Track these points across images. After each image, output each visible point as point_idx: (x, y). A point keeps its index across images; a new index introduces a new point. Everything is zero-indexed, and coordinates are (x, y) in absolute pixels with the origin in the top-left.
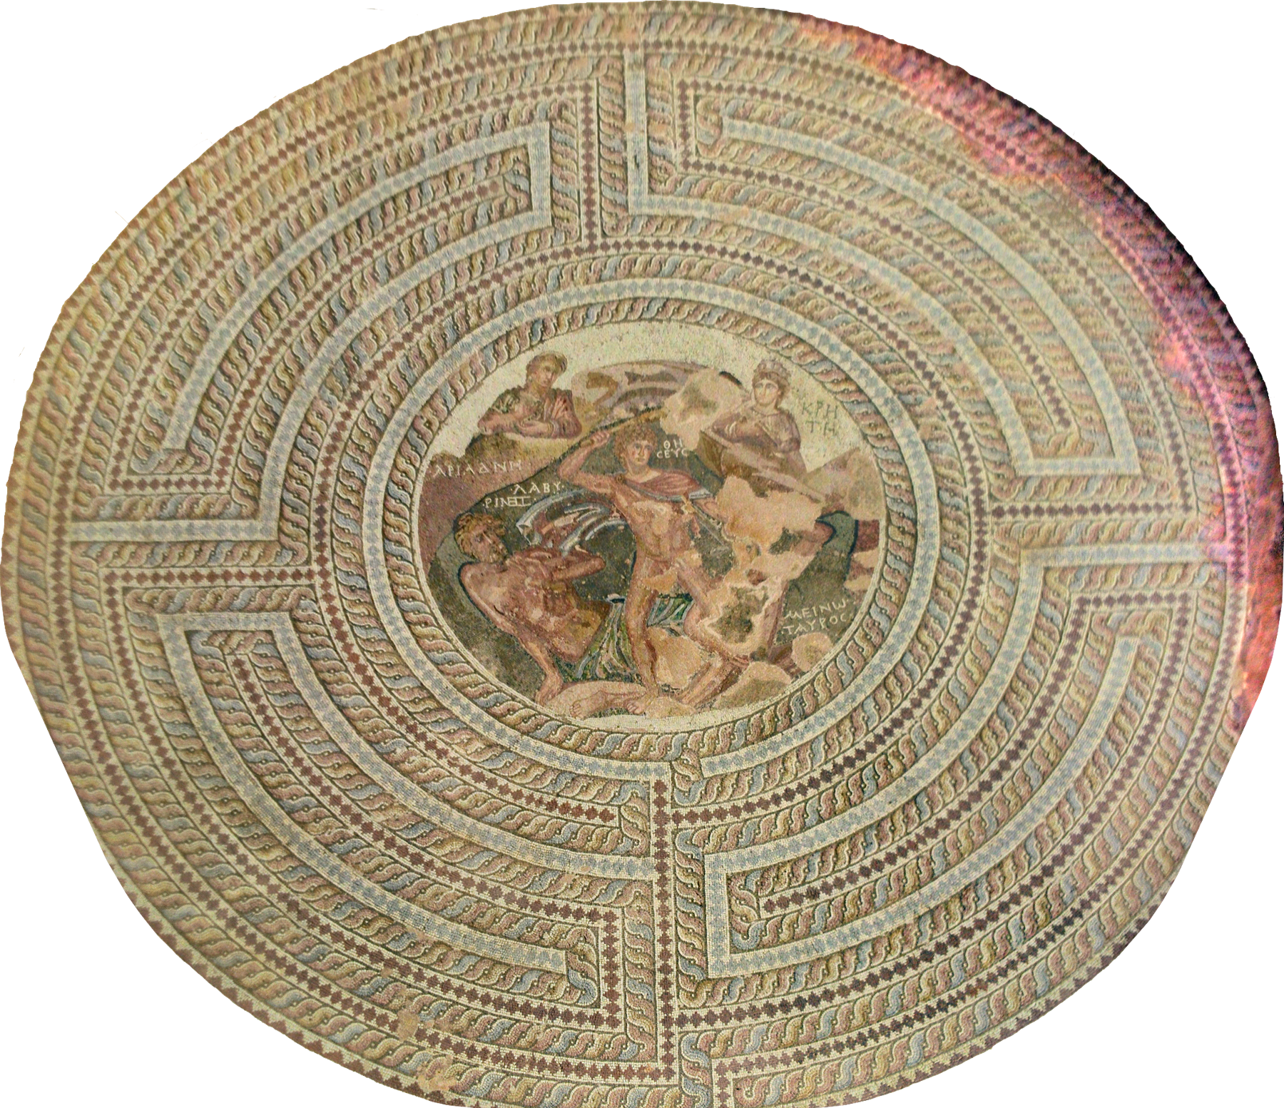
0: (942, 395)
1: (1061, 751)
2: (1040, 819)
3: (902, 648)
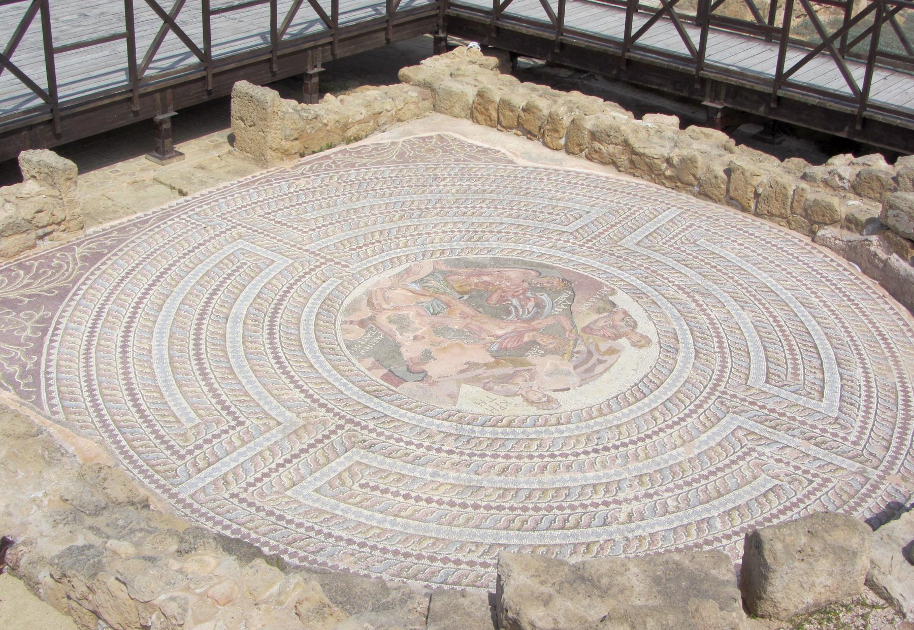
0: (450, 452)
1: (174, 369)
2: (154, 343)
3: (309, 356)
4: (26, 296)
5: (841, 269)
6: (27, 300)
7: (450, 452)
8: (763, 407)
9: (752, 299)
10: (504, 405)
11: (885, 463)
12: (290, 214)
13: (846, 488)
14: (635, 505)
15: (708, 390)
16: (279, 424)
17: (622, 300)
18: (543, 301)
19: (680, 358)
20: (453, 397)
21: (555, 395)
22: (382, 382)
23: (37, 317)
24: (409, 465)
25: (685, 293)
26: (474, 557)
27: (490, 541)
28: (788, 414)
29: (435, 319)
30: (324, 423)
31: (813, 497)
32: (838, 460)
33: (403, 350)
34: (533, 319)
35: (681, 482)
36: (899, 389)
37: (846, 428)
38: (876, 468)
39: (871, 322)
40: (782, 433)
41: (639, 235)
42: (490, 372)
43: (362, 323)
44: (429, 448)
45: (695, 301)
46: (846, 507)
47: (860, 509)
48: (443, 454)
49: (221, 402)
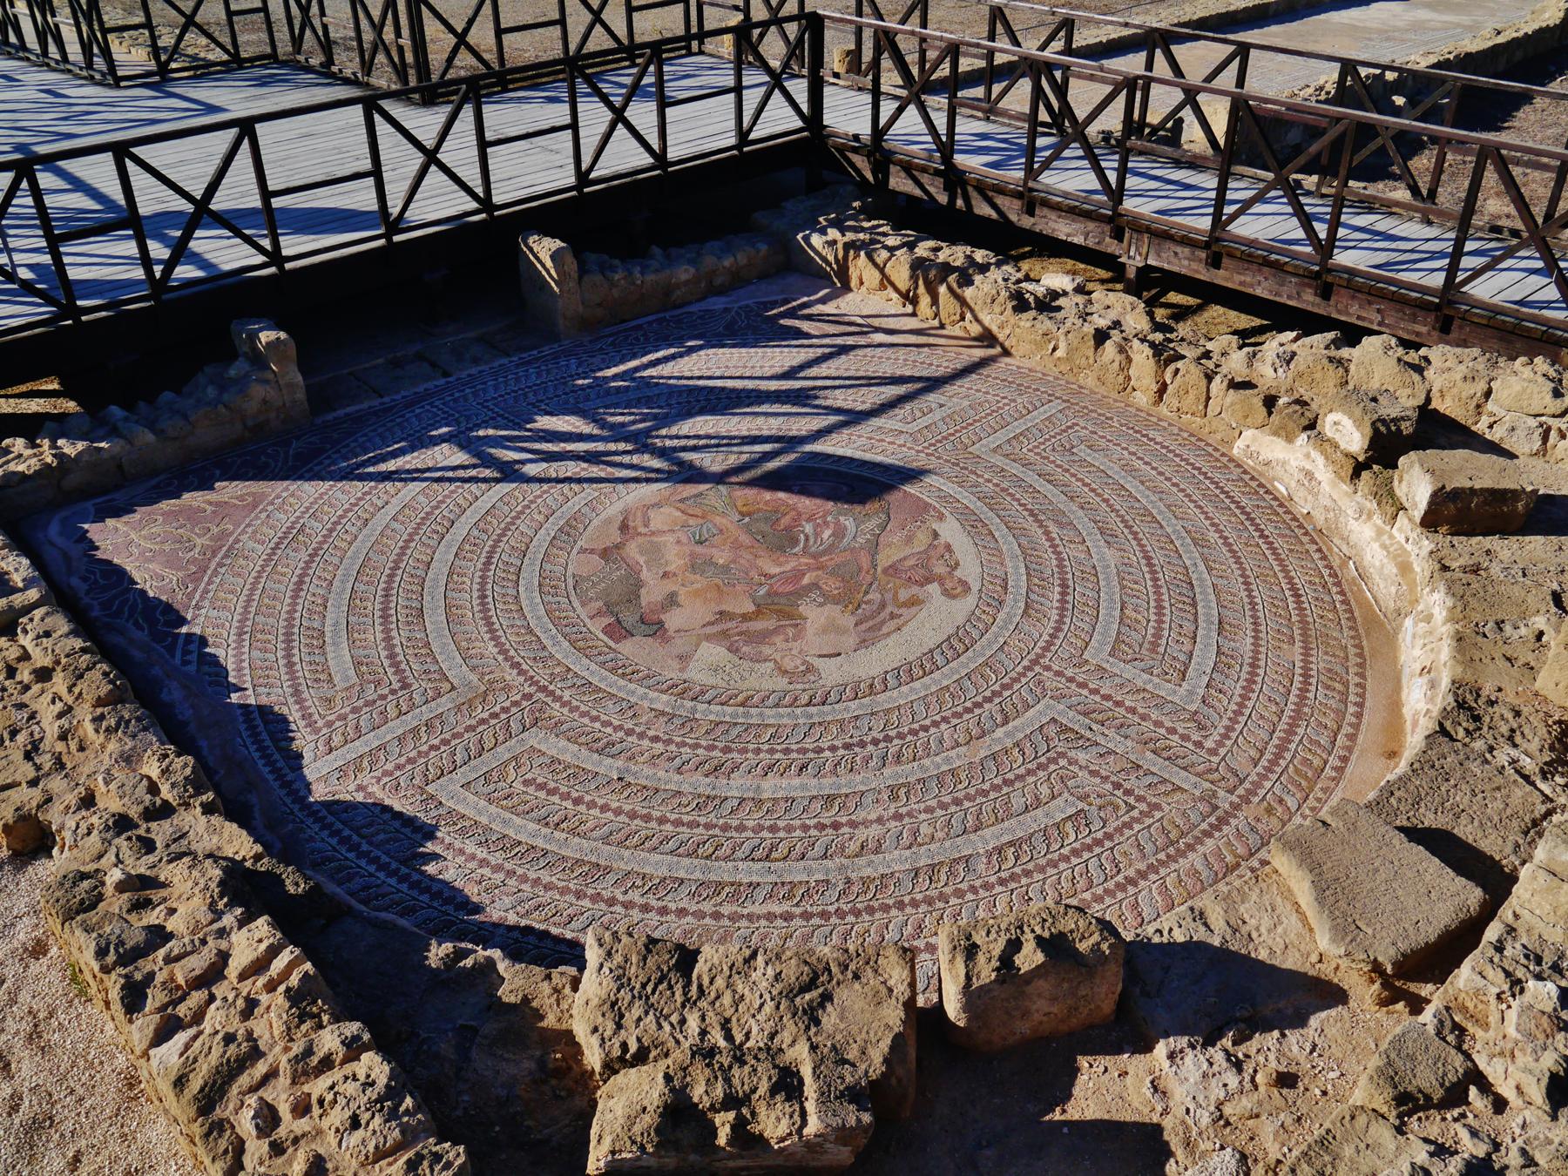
0: (656, 739)
4: (210, 503)
5: (1262, 491)
6: (209, 508)
7: (656, 739)
8: (1095, 692)
9: (1126, 531)
10: (746, 674)
11: (1247, 785)
12: (567, 402)
13: (1179, 821)
14: (875, 831)
15: (1025, 663)
16: (453, 688)
17: (950, 530)
18: (845, 528)
19: (1001, 616)
20: (684, 659)
21: (818, 663)
22: (601, 636)
23: (216, 530)
24: (596, 756)
25: (1037, 521)
26: (635, 896)
27: (663, 872)
28: (1128, 703)
29: (699, 549)
30: (507, 688)
31: (1127, 832)
32: (1180, 778)
33: (643, 591)
34: (824, 553)
35: (947, 799)
36: (1298, 671)
37: (1204, 728)
38: (1231, 792)
39: (1285, 570)
40: (1111, 733)
41: (1001, 437)
42: (744, 626)
43: (605, 554)
44: (630, 732)
45: (1047, 533)
46: (1171, 850)
47: (1191, 856)
48: (646, 743)
49: (392, 656)
